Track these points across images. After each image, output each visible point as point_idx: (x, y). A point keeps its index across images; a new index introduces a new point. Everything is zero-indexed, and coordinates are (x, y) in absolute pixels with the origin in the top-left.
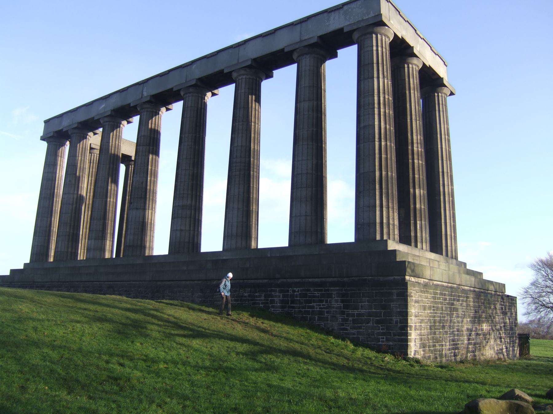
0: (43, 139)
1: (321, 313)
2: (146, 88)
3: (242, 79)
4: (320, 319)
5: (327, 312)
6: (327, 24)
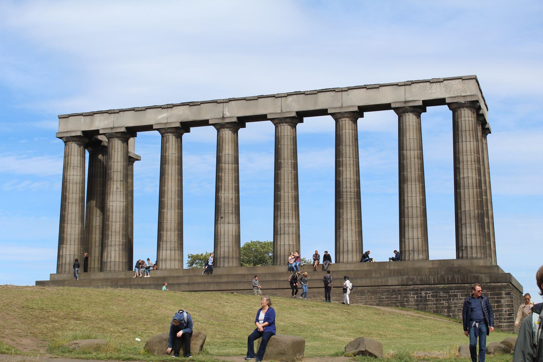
1: (449, 308)
2: (227, 108)
3: (345, 120)
5: (454, 307)
6: (430, 92)
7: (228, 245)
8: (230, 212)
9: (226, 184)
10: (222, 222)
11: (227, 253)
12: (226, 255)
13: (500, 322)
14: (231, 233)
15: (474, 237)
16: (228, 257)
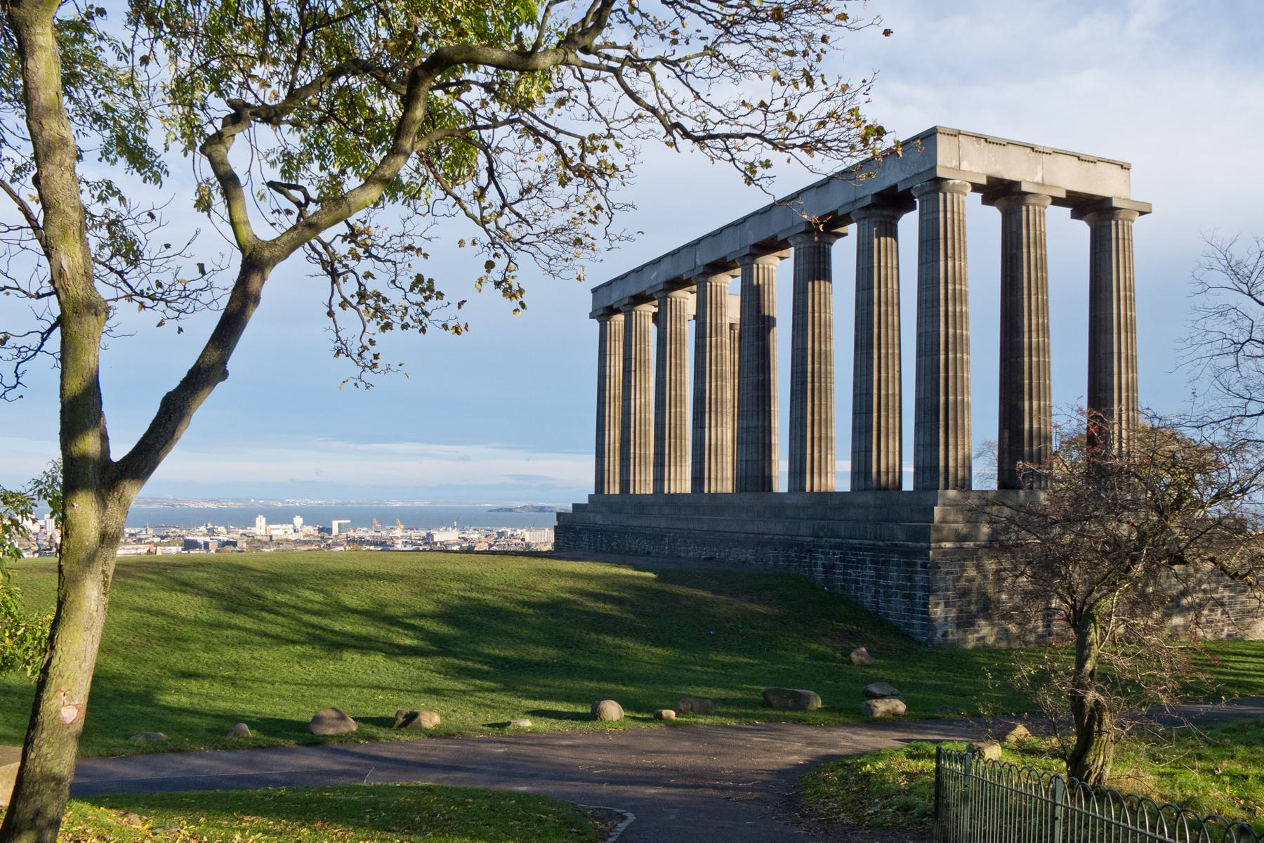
0: (592, 316)
1: (857, 582)
4: (858, 589)
5: (863, 581)
13: (913, 618)
15: (929, 448)
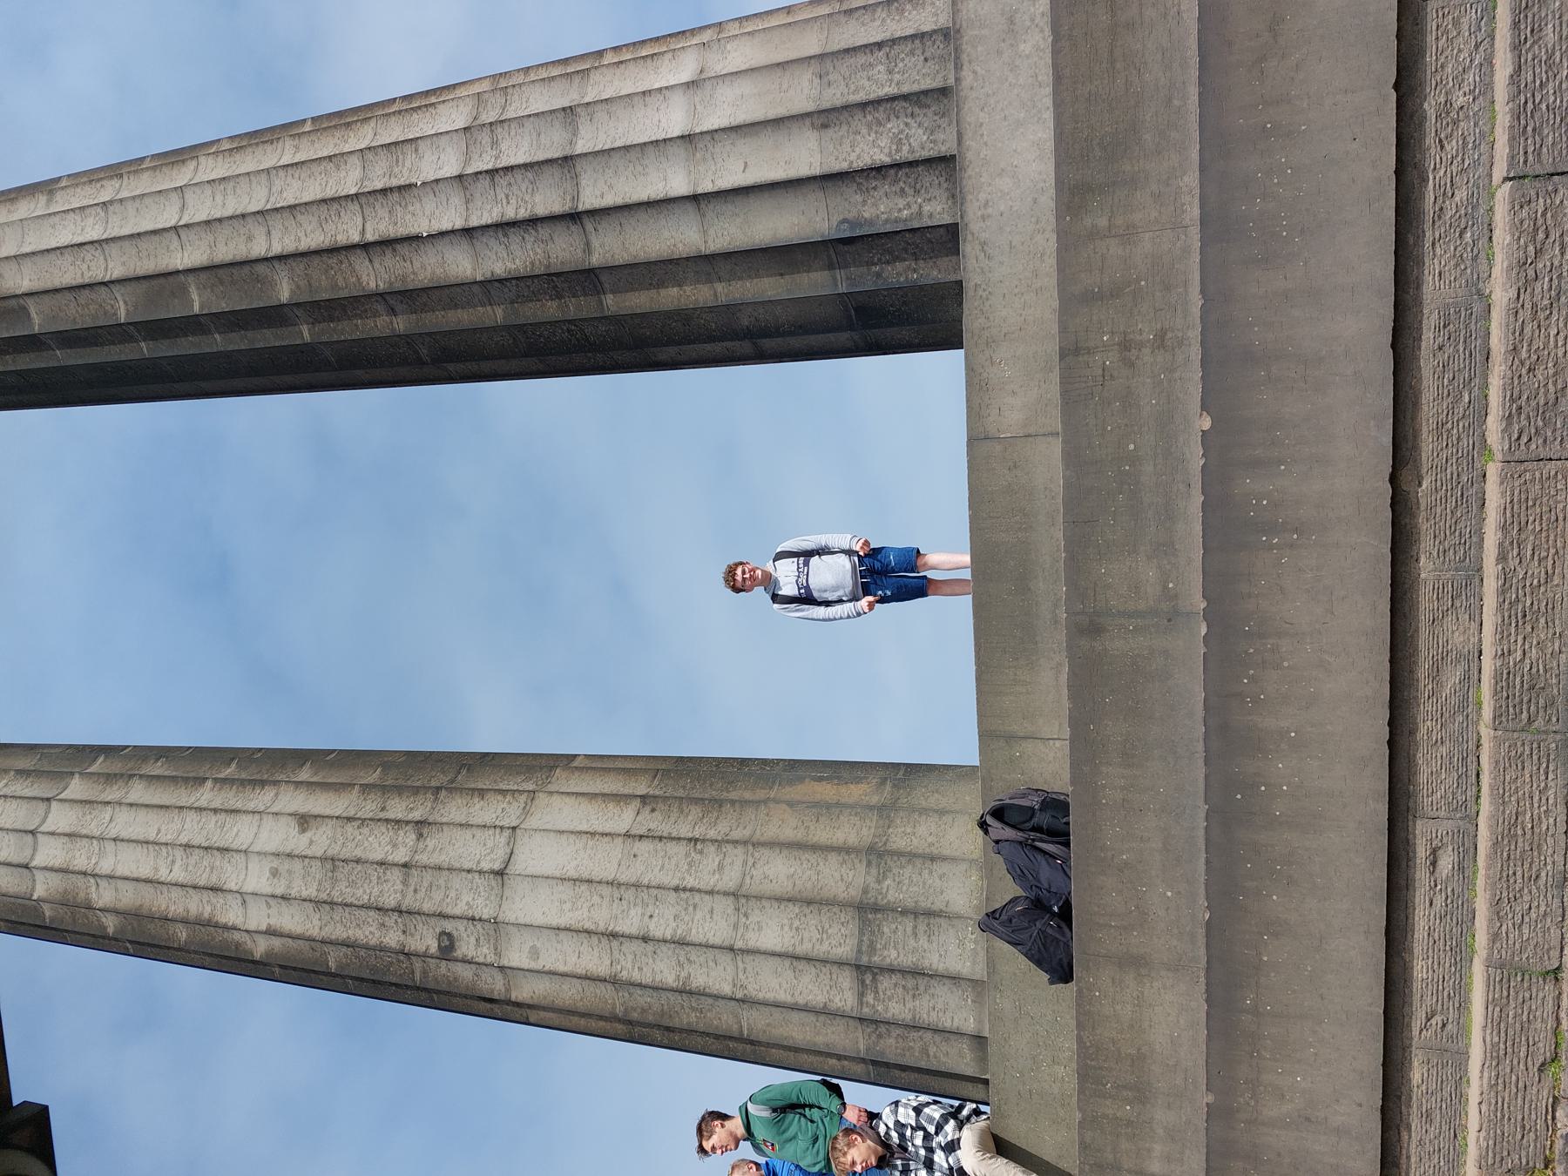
7: (724, 905)
8: (402, 847)
9: (178, 875)
10: (485, 953)
11: (813, 920)
12: (839, 939)
14: (605, 861)
16: (867, 910)
